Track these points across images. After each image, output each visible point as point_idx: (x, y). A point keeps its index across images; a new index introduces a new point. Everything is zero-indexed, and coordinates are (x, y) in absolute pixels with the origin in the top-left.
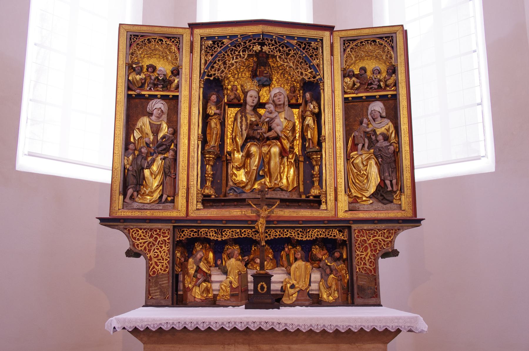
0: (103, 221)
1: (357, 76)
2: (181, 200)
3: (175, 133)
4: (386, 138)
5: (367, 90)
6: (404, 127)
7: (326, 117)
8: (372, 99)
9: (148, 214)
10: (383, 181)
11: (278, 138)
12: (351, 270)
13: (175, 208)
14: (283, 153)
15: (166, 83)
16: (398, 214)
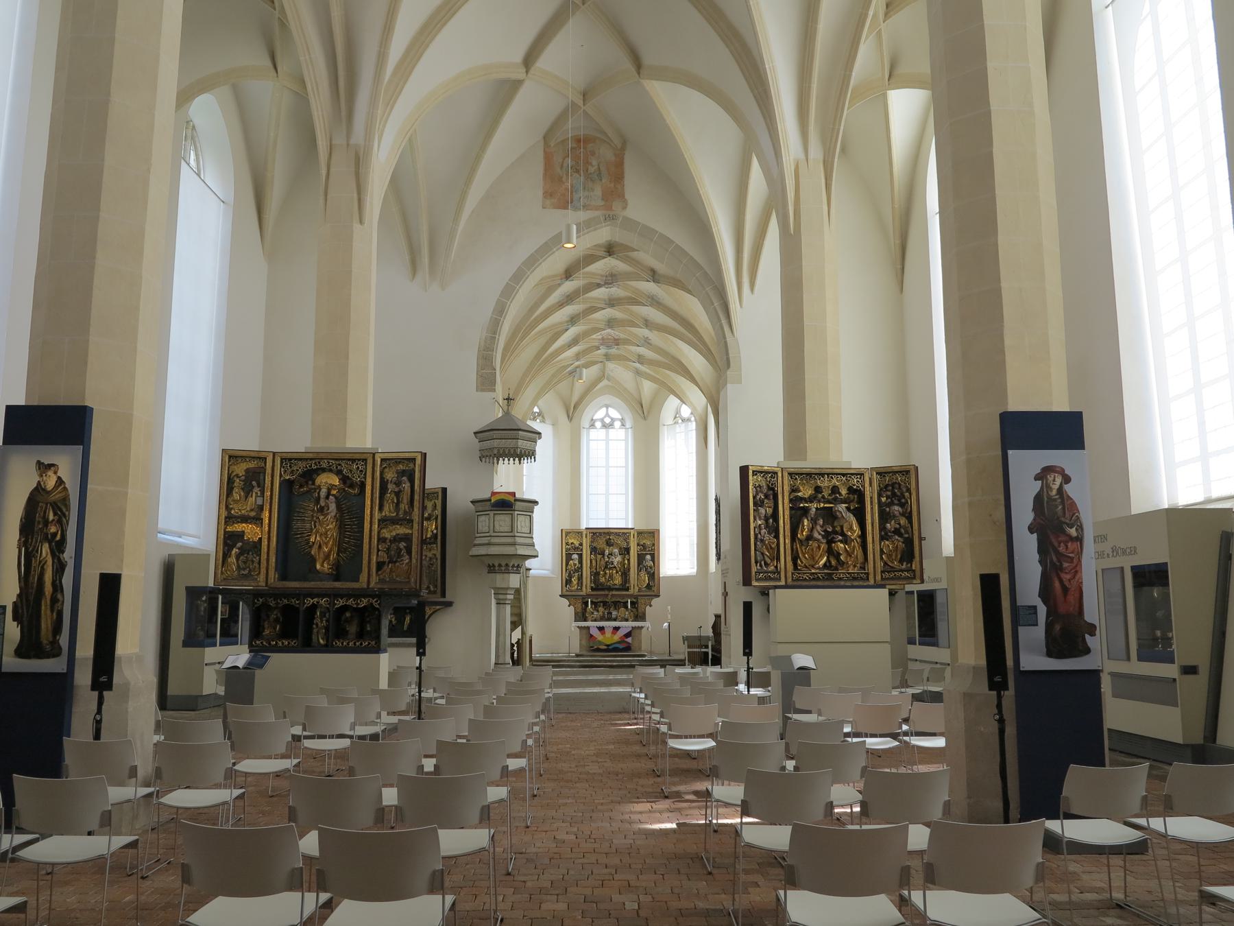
0: (560, 596)
1: (642, 545)
2: (584, 589)
3: (582, 566)
4: (651, 568)
5: (645, 551)
6: (656, 565)
7: (632, 560)
8: (647, 554)
9: (573, 593)
10: (649, 582)
11: (615, 567)
12: (637, 611)
13: (582, 591)
14: (617, 572)
15: (578, 548)
16: (653, 594)
